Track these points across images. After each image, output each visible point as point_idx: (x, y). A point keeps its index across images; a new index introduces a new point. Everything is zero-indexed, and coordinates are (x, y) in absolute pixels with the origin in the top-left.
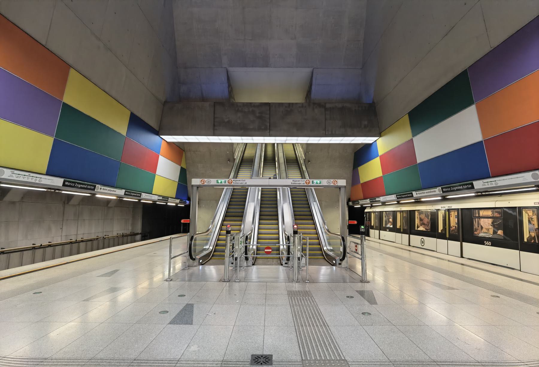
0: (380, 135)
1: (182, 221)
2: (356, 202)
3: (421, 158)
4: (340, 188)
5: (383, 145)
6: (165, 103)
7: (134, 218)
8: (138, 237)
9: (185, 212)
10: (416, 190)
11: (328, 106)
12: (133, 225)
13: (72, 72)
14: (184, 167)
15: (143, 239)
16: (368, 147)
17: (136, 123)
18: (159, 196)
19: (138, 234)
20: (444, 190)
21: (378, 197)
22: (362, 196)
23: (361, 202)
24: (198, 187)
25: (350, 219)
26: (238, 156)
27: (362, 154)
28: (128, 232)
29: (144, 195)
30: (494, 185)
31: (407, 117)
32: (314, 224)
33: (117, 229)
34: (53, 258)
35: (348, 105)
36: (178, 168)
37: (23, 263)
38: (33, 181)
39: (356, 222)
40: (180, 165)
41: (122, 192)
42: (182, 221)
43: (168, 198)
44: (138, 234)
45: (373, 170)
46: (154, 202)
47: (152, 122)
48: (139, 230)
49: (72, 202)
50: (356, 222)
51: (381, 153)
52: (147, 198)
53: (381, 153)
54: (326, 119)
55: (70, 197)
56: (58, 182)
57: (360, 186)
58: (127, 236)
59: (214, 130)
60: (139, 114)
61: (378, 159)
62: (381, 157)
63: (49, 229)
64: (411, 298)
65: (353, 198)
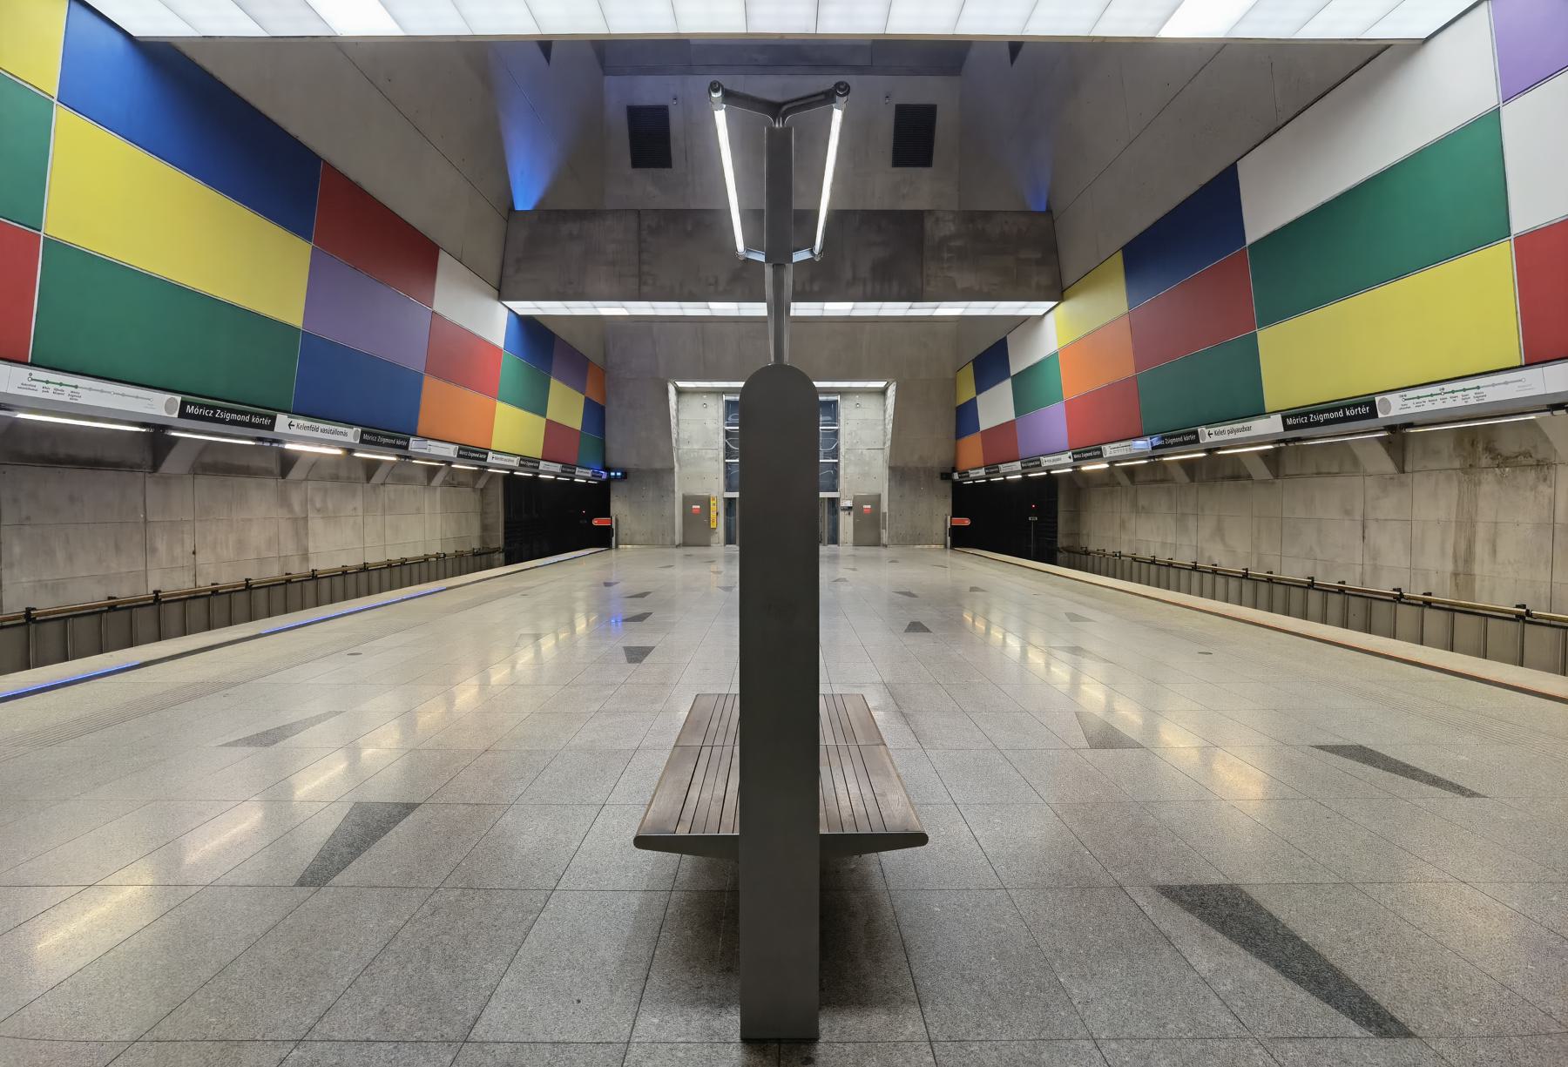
9: (598, 497)
65: (962, 466)
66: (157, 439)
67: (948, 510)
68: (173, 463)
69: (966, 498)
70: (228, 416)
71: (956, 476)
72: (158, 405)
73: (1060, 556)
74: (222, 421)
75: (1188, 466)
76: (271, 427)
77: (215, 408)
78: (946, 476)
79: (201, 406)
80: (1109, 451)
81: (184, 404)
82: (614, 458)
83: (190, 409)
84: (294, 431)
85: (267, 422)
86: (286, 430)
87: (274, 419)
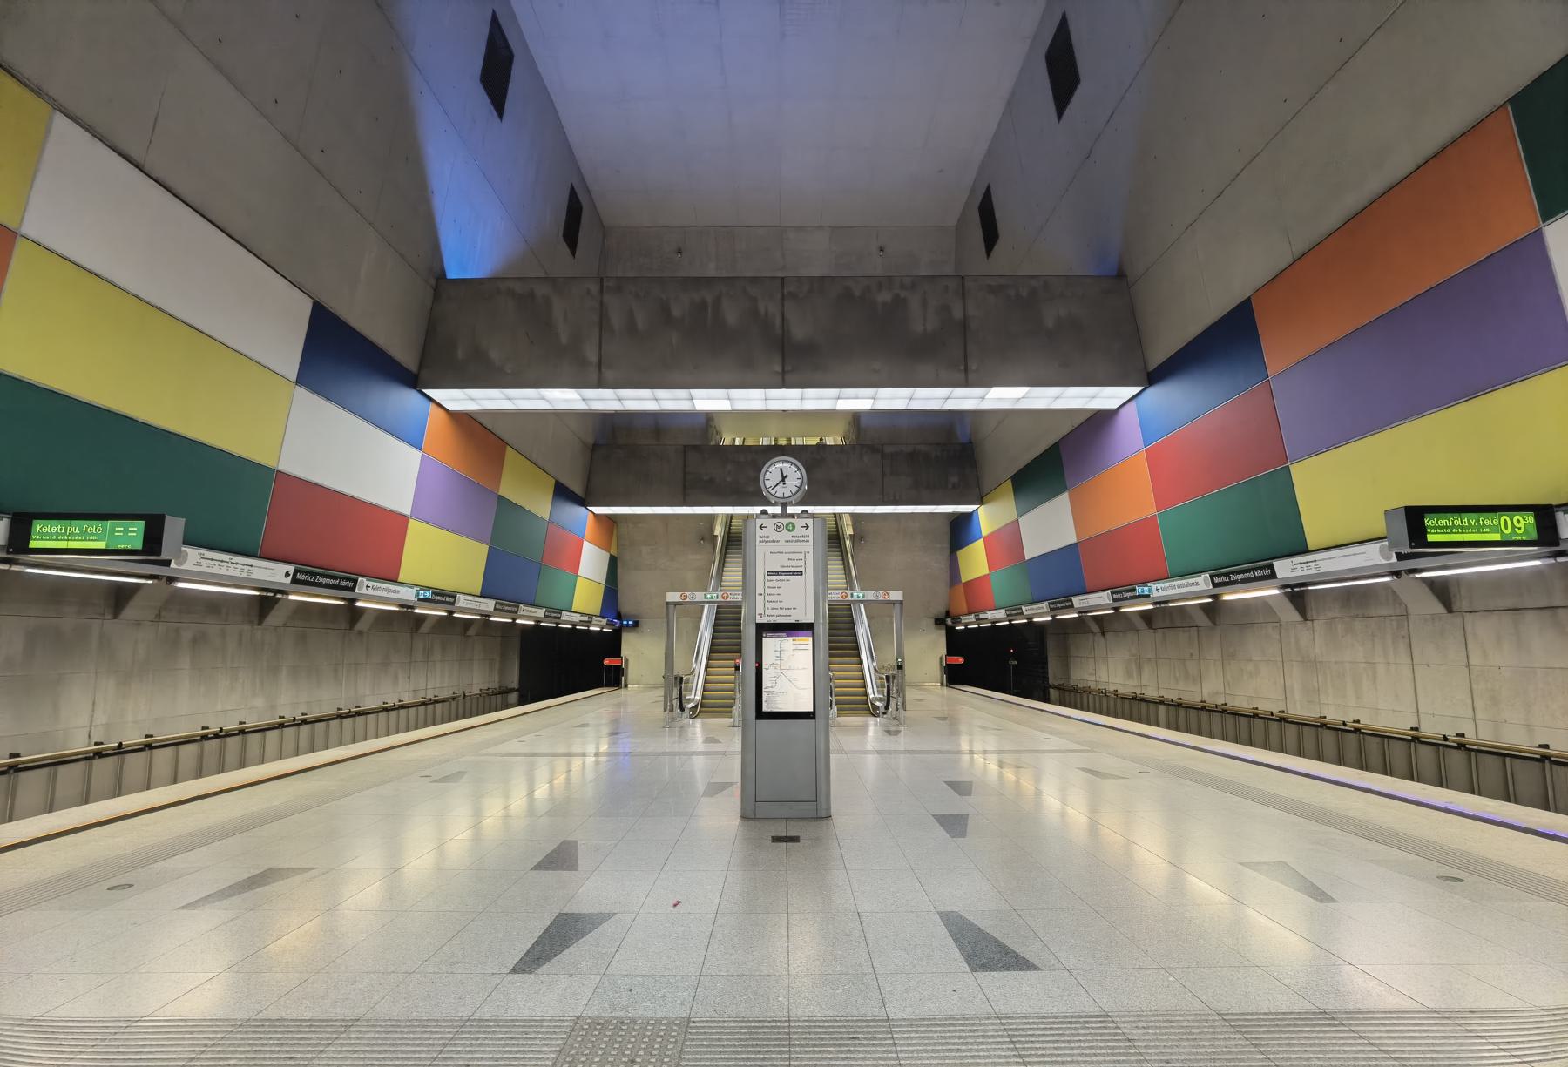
0: (981, 503)
1: (606, 662)
2: (957, 620)
3: (1030, 552)
4: (894, 603)
5: (988, 517)
6: (595, 447)
7: (504, 656)
8: (514, 697)
9: (612, 643)
10: (1026, 604)
11: (888, 449)
12: (502, 672)
13: (509, 450)
14: (614, 552)
15: (521, 702)
16: (968, 517)
17: (562, 493)
18: (583, 614)
19: (512, 690)
20: (1217, 580)
21: (985, 611)
22: (965, 609)
23: (965, 619)
24: (676, 604)
25: (949, 653)
26: (719, 531)
27: (959, 531)
28: (495, 685)
29: (565, 616)
30: (1313, 571)
31: (1009, 482)
32: (860, 662)
33: (478, 680)
34: (221, 770)
35: (923, 448)
36: (606, 556)
37: (180, 776)
38: (237, 574)
39: (961, 660)
40: (607, 549)
41: (541, 613)
42: (606, 662)
43: (591, 616)
44: (512, 690)
45: (975, 561)
46: (574, 625)
47: (577, 488)
48: (515, 685)
49: (425, 628)
50: (961, 660)
51: (985, 533)
52: (567, 619)
53: (985, 533)
54: (884, 474)
55: (423, 618)
56: (489, 605)
57: (961, 588)
58: (495, 693)
59: (685, 495)
60: (564, 481)
61: (980, 544)
62: (987, 540)
63: (396, 677)
64: (1027, 785)
65: (953, 612)
66: (266, 602)
67: (944, 651)
68: (275, 618)
69: (956, 642)
70: (325, 581)
71: (949, 621)
72: (276, 573)
73: (1053, 693)
74: (319, 585)
75: (1146, 616)
76: (352, 589)
77: (315, 574)
78: (939, 622)
79: (307, 573)
80: (1076, 600)
81: (296, 571)
82: (626, 606)
83: (300, 576)
84: (370, 592)
85: (350, 584)
86: (364, 591)
87: (355, 581)
